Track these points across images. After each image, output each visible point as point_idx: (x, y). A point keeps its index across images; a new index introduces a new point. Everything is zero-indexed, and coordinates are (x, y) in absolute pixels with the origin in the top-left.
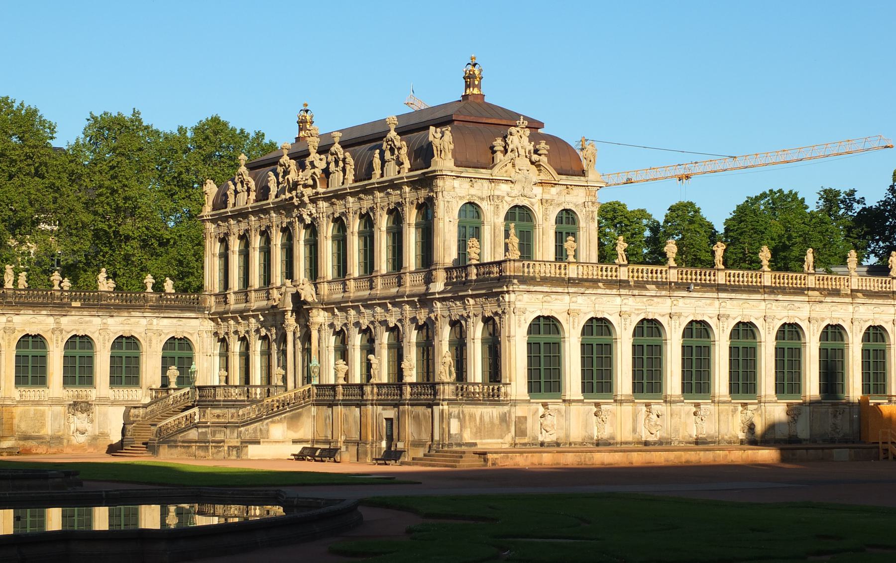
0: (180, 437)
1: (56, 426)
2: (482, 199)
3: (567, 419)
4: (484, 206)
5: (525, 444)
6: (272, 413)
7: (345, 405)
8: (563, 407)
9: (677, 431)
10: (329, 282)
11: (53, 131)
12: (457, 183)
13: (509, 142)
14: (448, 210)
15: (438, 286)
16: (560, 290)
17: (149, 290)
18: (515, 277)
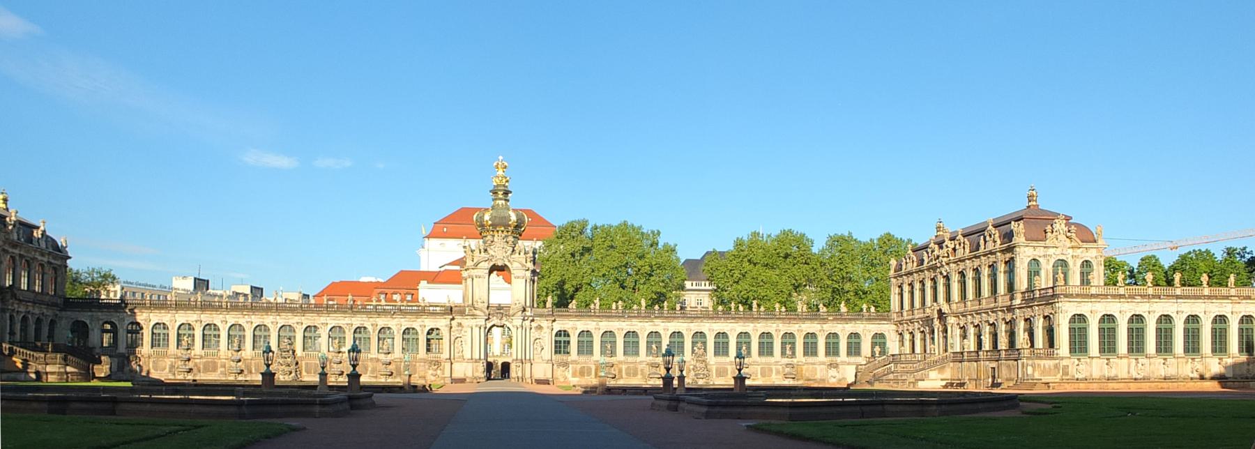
0: (884, 378)
3: (1091, 366)
5: (1068, 379)
6: (932, 365)
8: (1088, 360)
10: (956, 303)
11: (812, 243)
15: (1017, 301)
17: (865, 311)
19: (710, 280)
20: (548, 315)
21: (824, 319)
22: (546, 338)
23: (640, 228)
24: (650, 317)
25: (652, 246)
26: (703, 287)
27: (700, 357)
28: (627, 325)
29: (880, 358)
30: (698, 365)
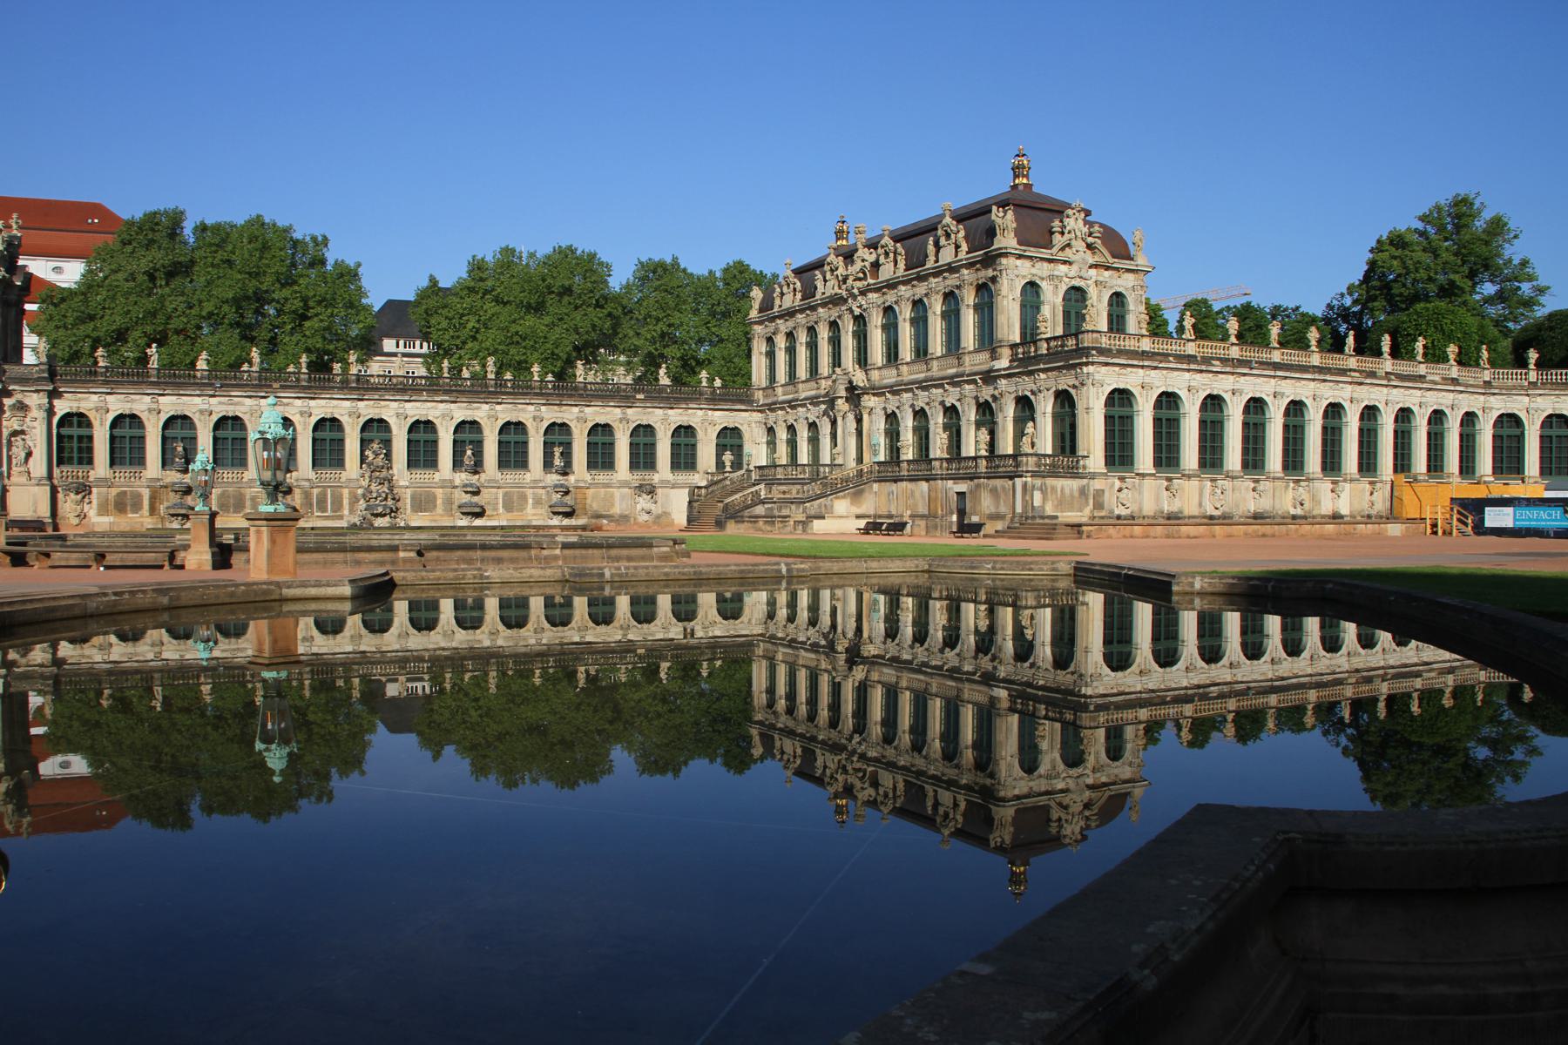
0: (746, 513)
1: (624, 506)
2: (1043, 279)
4: (1044, 284)
5: (1102, 518)
6: (835, 488)
7: (911, 480)
9: (1237, 506)
10: (879, 368)
12: (1019, 262)
13: (1066, 223)
14: (1011, 289)
15: (1003, 363)
16: (1135, 362)
17: (704, 384)
18: (1093, 348)
19: (426, 337)
20: (39, 379)
21: (627, 397)
22: (39, 428)
23: (287, 230)
24: (271, 386)
25: (312, 265)
26: (417, 350)
27: (379, 471)
28: (220, 403)
29: (732, 475)
30: (374, 487)
